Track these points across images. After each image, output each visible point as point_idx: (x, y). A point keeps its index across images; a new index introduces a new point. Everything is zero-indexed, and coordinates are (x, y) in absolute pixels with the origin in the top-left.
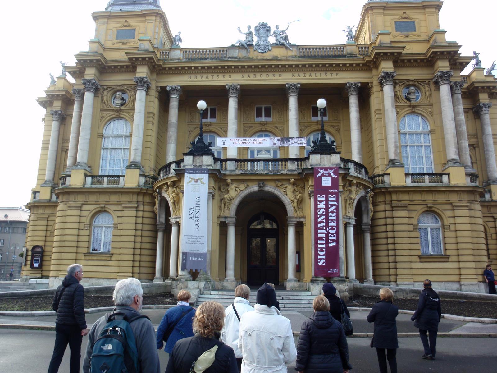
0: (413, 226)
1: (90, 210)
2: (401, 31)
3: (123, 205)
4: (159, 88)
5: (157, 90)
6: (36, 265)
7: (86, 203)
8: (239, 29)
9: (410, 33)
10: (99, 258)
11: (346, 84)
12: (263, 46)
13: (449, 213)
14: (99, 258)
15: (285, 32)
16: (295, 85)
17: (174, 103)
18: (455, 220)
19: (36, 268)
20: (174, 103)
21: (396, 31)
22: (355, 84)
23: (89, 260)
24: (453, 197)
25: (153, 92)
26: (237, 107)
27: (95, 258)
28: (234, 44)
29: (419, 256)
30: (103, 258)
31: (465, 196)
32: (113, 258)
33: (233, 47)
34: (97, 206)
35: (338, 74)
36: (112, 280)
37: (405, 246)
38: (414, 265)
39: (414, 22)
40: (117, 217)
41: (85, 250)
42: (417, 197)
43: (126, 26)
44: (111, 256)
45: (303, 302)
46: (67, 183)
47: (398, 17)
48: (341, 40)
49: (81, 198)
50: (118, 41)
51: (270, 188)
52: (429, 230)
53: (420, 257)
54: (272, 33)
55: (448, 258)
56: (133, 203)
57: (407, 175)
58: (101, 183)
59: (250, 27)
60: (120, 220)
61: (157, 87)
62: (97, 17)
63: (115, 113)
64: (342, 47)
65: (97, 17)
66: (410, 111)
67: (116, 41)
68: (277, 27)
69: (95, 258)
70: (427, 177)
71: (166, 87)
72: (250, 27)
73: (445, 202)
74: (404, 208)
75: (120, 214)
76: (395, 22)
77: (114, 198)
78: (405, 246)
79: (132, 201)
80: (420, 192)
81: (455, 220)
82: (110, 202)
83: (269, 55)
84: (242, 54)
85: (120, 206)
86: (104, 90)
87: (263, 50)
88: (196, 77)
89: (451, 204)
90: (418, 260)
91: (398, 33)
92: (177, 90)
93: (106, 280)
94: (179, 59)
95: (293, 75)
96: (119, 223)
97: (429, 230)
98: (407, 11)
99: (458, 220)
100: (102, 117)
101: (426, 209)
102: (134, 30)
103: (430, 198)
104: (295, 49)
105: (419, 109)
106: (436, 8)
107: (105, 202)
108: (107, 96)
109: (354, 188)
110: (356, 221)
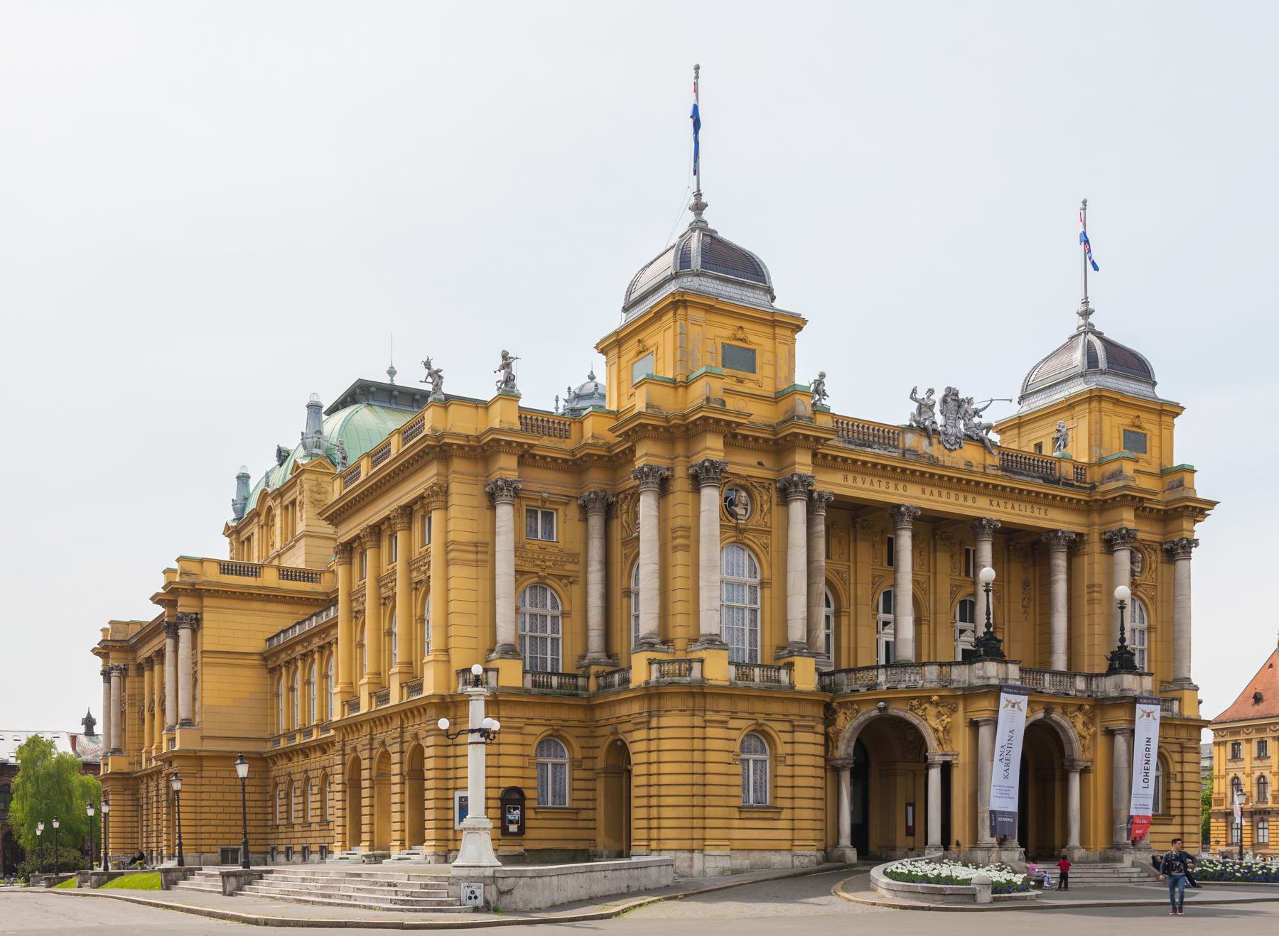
1: (740, 729)
3: (795, 723)
6: (513, 828)
7: (734, 715)
8: (914, 391)
10: (762, 815)
12: (953, 438)
13: (1177, 757)
14: (762, 815)
15: (981, 413)
18: (1182, 767)
19: (513, 834)
23: (747, 819)
27: (756, 815)
30: (768, 815)
32: (786, 814)
34: (751, 722)
35: (1048, 512)
36: (782, 852)
40: (785, 743)
41: (739, 802)
44: (780, 812)
46: (696, 673)
49: (724, 704)
56: (807, 718)
58: (746, 677)
59: (931, 391)
60: (788, 749)
63: (733, 533)
69: (756, 815)
72: (931, 391)
75: (787, 737)
77: (776, 708)
79: (804, 716)
81: (1182, 767)
82: (773, 716)
85: (786, 724)
87: (952, 445)
89: (1181, 744)
93: (773, 852)
96: (787, 754)
107: (763, 716)
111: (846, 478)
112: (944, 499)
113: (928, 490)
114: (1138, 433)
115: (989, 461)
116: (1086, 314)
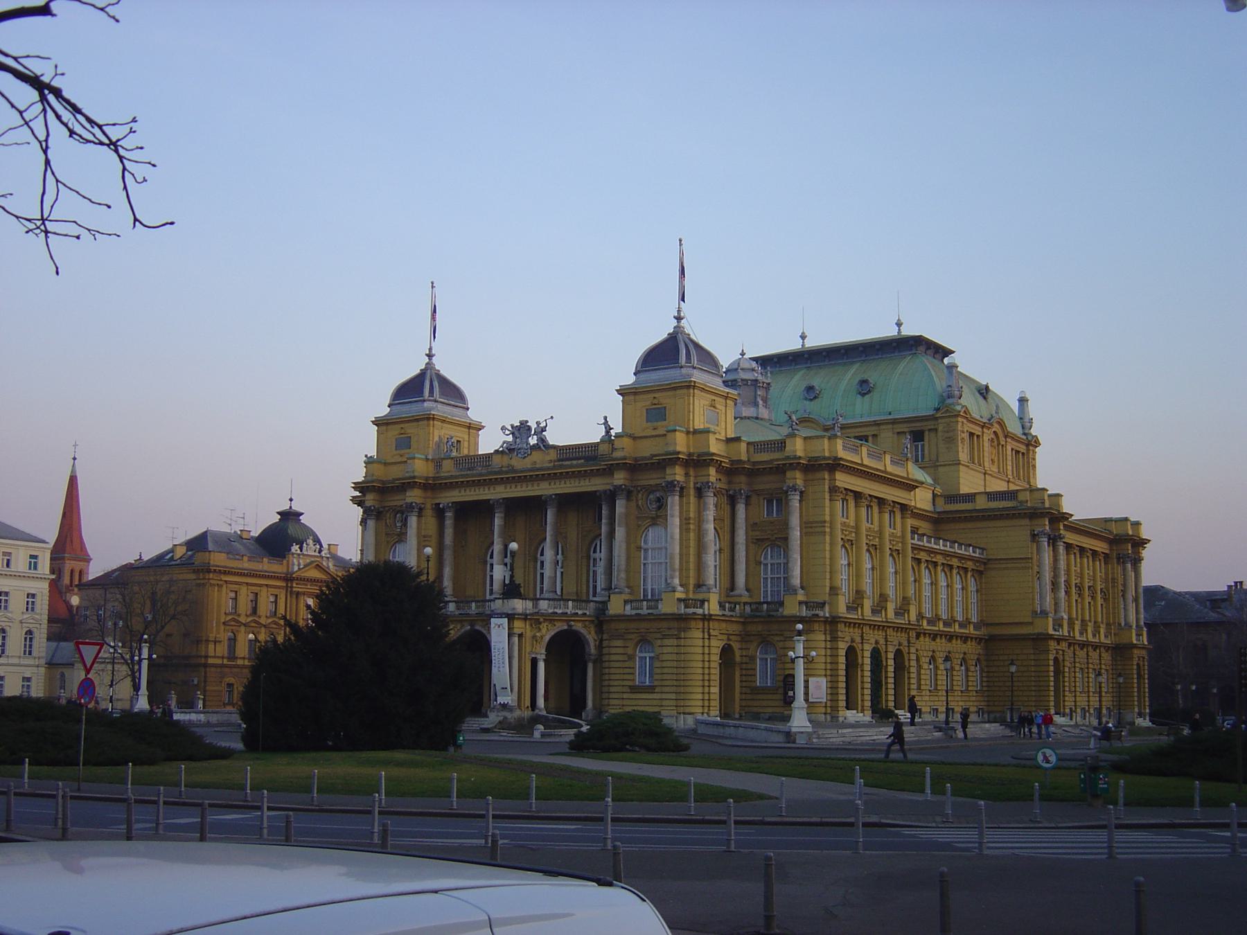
0: (628, 656)
2: (651, 422)
4: (434, 506)
5: (432, 509)
9: (659, 424)
11: (596, 491)
16: (551, 496)
17: (449, 522)
20: (449, 522)
21: (647, 422)
22: (605, 491)
24: (665, 625)
25: (429, 512)
26: (503, 523)
28: (496, 448)
29: (630, 686)
31: (675, 624)
33: (497, 451)
37: (618, 677)
38: (625, 696)
39: (665, 408)
42: (633, 625)
43: (402, 434)
45: (475, 725)
47: (649, 403)
48: (594, 435)
50: (398, 452)
51: (478, 628)
52: (648, 658)
53: (630, 687)
54: (533, 432)
55: (655, 689)
57: (626, 602)
61: (432, 504)
62: (378, 422)
64: (596, 445)
65: (378, 422)
66: (651, 523)
67: (395, 452)
68: (538, 423)
70: (645, 603)
71: (439, 504)
73: (656, 630)
74: (621, 637)
76: (647, 410)
78: (618, 677)
80: (640, 620)
83: (527, 463)
84: (505, 460)
86: (387, 511)
88: (465, 490)
90: (629, 691)
91: (649, 424)
92: (450, 507)
94: (449, 472)
95: (550, 484)
97: (648, 658)
98: (656, 395)
99: (665, 650)
100: (388, 542)
101: (640, 638)
102: (410, 437)
103: (644, 625)
104: (552, 451)
105: (660, 520)
106: (687, 388)
108: (390, 519)
109: (544, 626)
110: (546, 655)
111: (460, 492)
112: (524, 488)
113: (508, 486)
114: (659, 408)
115: (548, 458)
116: (679, 318)
